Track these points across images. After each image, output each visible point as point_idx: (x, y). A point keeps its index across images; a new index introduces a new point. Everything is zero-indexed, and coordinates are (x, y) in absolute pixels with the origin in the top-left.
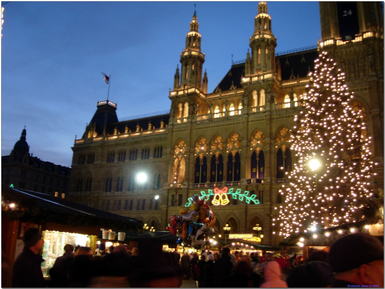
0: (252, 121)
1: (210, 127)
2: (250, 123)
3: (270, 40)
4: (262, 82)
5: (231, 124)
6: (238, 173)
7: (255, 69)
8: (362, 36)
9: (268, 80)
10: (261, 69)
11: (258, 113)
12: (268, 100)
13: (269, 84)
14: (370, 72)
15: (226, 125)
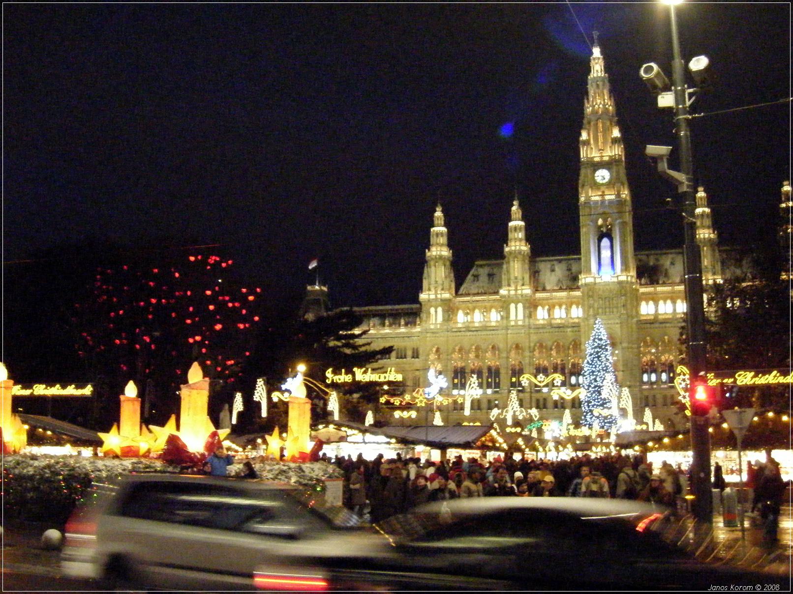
0: (511, 333)
2: (509, 335)
3: (526, 252)
4: (520, 296)
5: (490, 335)
8: (617, 277)
9: (526, 295)
10: (518, 282)
11: (516, 326)
12: (526, 315)
14: (623, 310)
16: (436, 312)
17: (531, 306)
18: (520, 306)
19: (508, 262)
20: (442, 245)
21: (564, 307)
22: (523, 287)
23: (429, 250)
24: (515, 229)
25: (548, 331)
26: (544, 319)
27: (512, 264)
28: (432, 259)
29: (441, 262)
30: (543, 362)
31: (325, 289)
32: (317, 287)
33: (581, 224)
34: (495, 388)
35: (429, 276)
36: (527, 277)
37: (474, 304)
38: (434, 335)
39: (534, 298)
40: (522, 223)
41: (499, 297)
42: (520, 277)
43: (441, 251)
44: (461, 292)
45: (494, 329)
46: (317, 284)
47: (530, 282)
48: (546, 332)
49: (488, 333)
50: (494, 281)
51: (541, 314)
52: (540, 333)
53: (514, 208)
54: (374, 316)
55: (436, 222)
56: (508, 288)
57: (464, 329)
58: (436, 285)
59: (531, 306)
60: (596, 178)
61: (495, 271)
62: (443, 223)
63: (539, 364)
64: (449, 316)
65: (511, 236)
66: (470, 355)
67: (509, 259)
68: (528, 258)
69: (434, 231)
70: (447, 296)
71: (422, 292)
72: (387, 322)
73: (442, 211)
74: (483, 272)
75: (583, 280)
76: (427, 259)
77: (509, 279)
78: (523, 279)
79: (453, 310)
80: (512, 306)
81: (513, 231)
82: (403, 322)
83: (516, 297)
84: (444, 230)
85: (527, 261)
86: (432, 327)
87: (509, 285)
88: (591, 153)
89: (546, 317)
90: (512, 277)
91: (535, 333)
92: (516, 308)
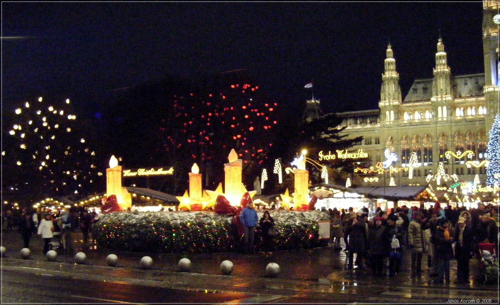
0: (439, 126)
1: (410, 128)
2: (438, 127)
5: (425, 127)
6: (431, 157)
7: (439, 92)
9: (449, 101)
11: (443, 121)
12: (449, 114)
13: (449, 104)
15: (421, 128)
16: (390, 114)
17: (452, 108)
18: (445, 108)
19: (436, 80)
20: (392, 70)
21: (474, 108)
22: (446, 96)
23: (384, 74)
24: (440, 57)
25: (464, 124)
26: (460, 116)
27: (438, 80)
28: (386, 80)
29: (392, 82)
30: (461, 144)
31: (318, 102)
32: (313, 101)
33: (484, 52)
34: (429, 162)
35: (384, 91)
36: (449, 88)
37: (415, 108)
38: (389, 129)
39: (454, 103)
40: (445, 54)
41: (430, 102)
42: (444, 89)
43: (392, 74)
44: (405, 100)
45: (428, 123)
46: (313, 99)
47: (451, 92)
48: (462, 125)
49: (425, 126)
50: (427, 92)
51: (459, 113)
52: (458, 125)
53: (439, 44)
54: (350, 118)
55: (388, 55)
56: (436, 97)
57: (408, 125)
58: (389, 97)
59: (452, 108)
60: (494, 21)
61: (428, 86)
62: (392, 55)
63: (458, 146)
64: (398, 116)
65: (437, 62)
66: (413, 141)
67: (436, 78)
68: (449, 76)
69: (387, 61)
70: (396, 103)
71: (380, 102)
72: (358, 122)
73: (392, 48)
74: (420, 87)
75: (486, 90)
76: (383, 79)
77: (437, 91)
78: (446, 90)
79: (401, 112)
80: (440, 108)
81: (439, 59)
82: (368, 121)
83: (442, 102)
84: (393, 60)
85: (448, 78)
86: (388, 123)
87: (437, 95)
88: (490, 4)
89: (462, 115)
90: (439, 90)
91: (455, 125)
92: (442, 109)
